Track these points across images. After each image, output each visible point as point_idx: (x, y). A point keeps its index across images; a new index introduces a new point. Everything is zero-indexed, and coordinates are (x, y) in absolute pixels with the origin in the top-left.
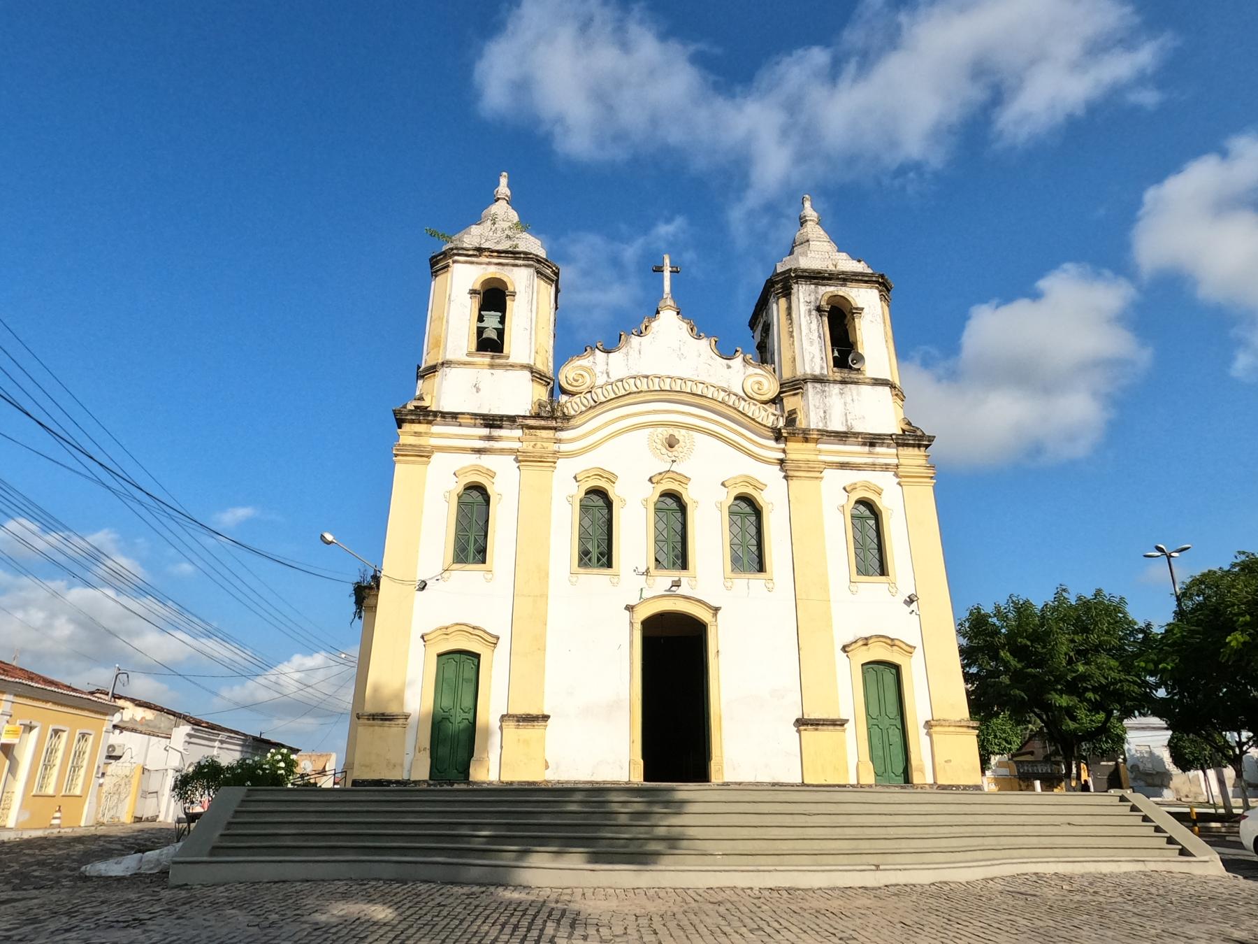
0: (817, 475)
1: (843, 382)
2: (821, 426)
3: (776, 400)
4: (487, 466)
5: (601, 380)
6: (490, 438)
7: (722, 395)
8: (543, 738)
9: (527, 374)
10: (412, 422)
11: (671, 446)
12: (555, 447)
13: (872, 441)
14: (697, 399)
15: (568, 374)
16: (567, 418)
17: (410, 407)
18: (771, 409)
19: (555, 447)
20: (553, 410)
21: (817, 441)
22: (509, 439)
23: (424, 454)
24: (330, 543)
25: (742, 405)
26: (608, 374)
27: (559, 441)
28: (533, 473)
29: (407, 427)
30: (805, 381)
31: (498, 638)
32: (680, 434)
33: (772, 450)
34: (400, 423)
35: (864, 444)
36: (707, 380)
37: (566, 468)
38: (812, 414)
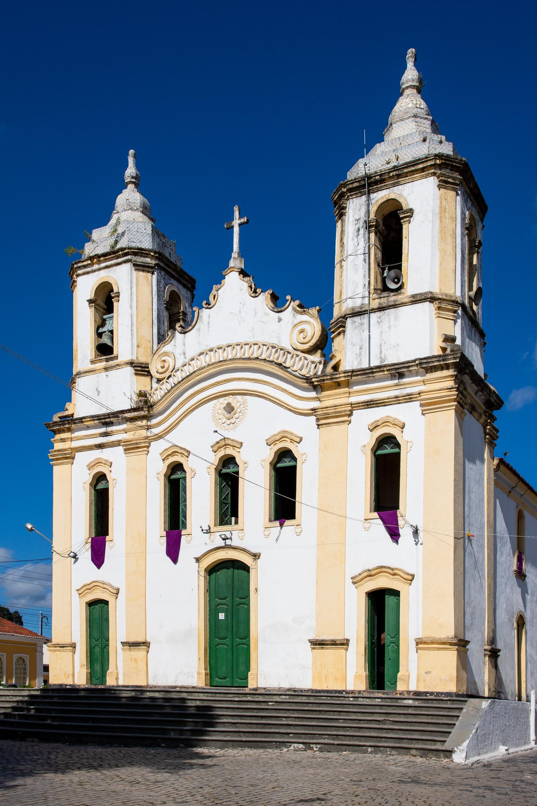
0: (346, 418)
1: (381, 309)
2: (355, 367)
6: (106, 434)
9: (130, 370)
13: (398, 371)
17: (56, 418)
18: (317, 357)
21: (348, 384)
22: (118, 432)
27: (148, 428)
29: (58, 437)
30: (345, 317)
33: (307, 400)
35: (393, 377)
36: (260, 339)
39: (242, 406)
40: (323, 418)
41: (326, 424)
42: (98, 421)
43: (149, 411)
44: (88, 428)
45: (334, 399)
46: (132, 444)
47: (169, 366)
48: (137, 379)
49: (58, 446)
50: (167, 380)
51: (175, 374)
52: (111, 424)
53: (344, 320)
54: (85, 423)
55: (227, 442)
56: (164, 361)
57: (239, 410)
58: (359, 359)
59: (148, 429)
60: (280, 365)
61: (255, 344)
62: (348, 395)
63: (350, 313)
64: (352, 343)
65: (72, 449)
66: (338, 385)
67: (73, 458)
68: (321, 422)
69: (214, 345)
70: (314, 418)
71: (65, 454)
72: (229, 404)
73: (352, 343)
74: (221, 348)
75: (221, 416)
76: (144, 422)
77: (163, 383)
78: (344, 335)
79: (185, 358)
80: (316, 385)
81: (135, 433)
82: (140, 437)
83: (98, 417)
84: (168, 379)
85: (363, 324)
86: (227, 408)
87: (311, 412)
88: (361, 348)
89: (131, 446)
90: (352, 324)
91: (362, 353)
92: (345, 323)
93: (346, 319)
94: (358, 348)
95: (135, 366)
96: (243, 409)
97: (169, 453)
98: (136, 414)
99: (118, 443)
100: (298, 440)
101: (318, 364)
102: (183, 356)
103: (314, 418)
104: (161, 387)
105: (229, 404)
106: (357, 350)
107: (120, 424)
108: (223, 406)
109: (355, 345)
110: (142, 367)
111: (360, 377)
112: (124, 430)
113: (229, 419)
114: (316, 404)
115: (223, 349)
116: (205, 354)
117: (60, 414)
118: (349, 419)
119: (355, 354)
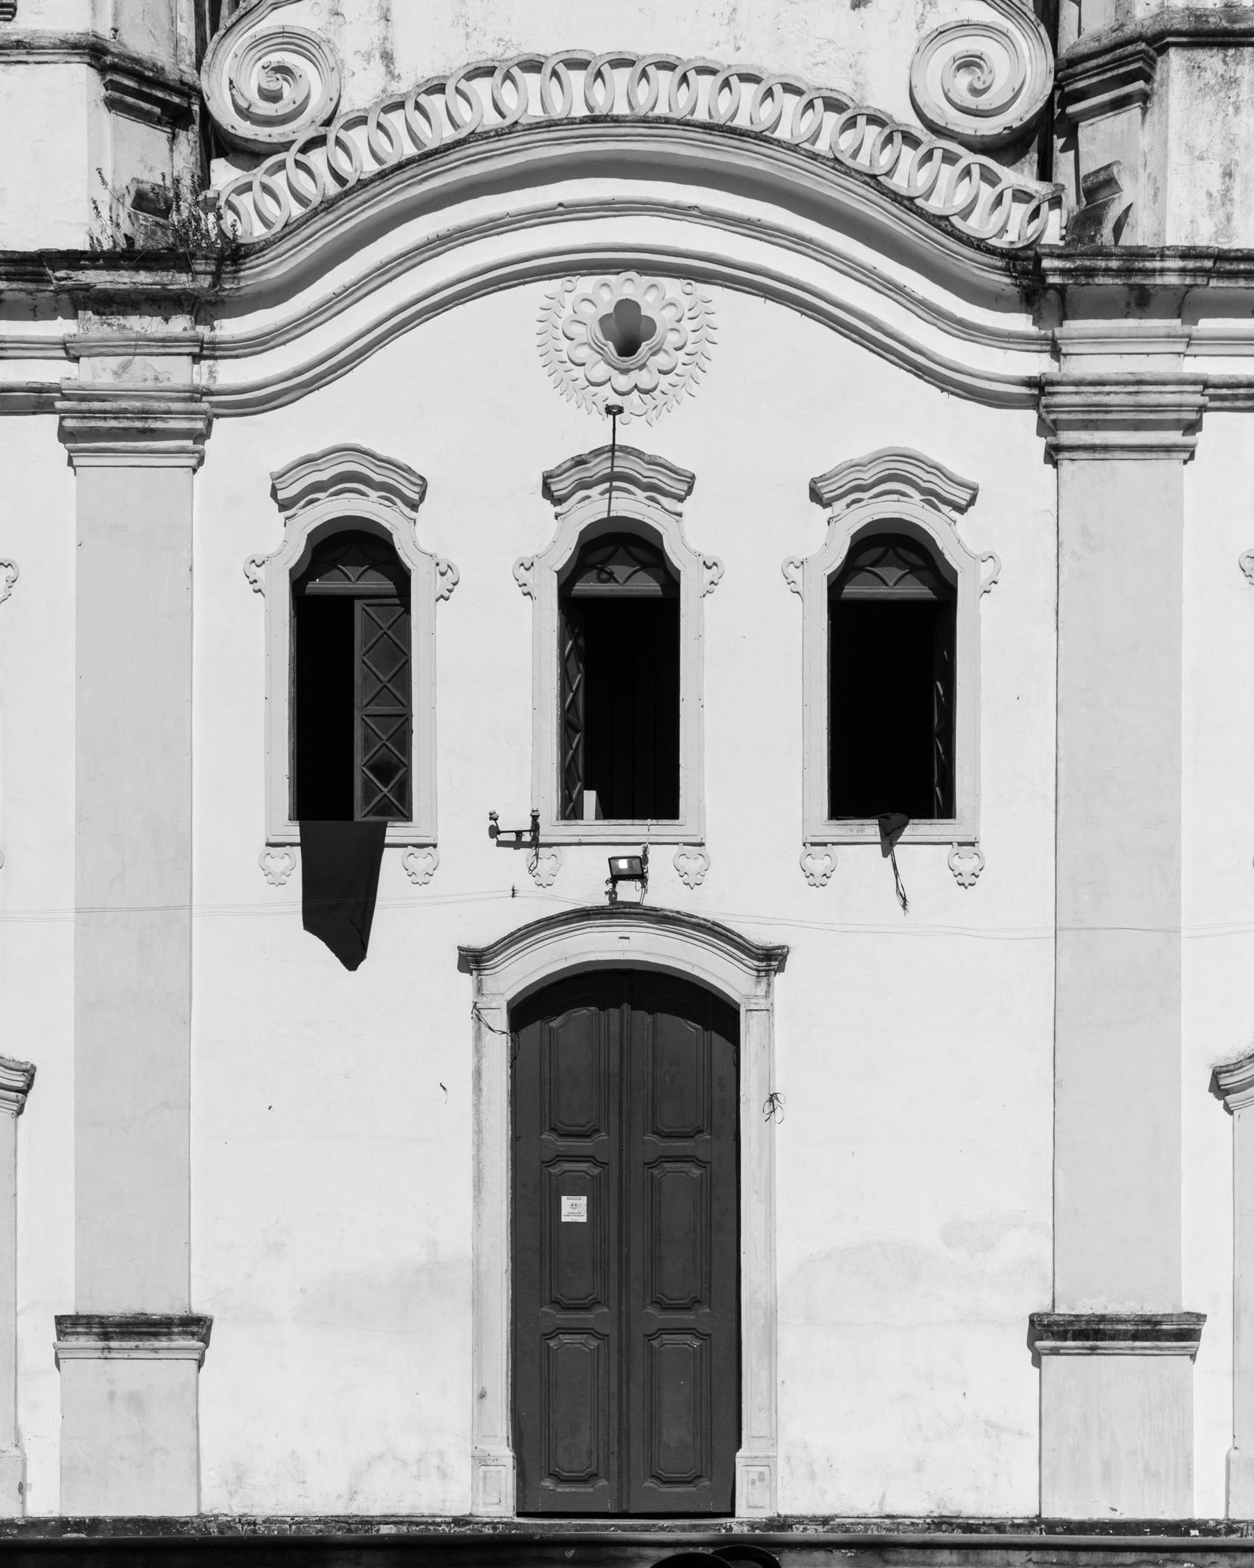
0: (1175, 437)
3: (1042, 135)
5: (361, 93)
7: (829, 134)
11: (628, 347)
12: (200, 375)
14: (720, 159)
15: (231, 82)
16: (234, 254)
18: (1022, 176)
19: (200, 375)
21: (1182, 305)
25: (909, 175)
26: (387, 57)
27: (204, 352)
28: (124, 479)
30: (1158, 42)
32: (658, 298)
36: (772, 65)
37: (248, 451)
38: (1176, 190)
39: (687, 325)
40: (1065, 422)
41: (1092, 448)
43: (217, 277)
45: (1108, 352)
46: (117, 414)
47: (308, 97)
48: (115, 128)
50: (300, 157)
51: (343, 135)
53: (1152, 52)
55: (624, 464)
56: (283, 70)
57: (673, 339)
58: (1221, 213)
59: (197, 358)
60: (872, 180)
61: (746, 78)
62: (1181, 348)
63: (1185, 27)
64: (1190, 148)
66: (1141, 301)
68: (1067, 437)
69: (547, 45)
70: (1031, 416)
72: (627, 308)
73: (1190, 148)
74: (582, 65)
75: (583, 353)
76: (180, 324)
77: (281, 166)
78: (1145, 111)
79: (394, 77)
80: (1030, 282)
81: (125, 367)
82: (150, 384)
84: (304, 149)
85: (1234, 82)
86: (612, 323)
87: (1024, 390)
88: (1228, 174)
90: (1189, 73)
91: (1236, 193)
92: (1152, 63)
93: (1163, 50)
94: (1217, 171)
95: (114, 68)
96: (692, 337)
97: (324, 476)
98: (144, 278)
100: (963, 496)
101: (1045, 206)
102: (378, 65)
103: (1031, 416)
104: (267, 180)
105: (627, 308)
106: (1216, 186)
107: (35, 313)
108: (592, 314)
109: (1201, 159)
110: (139, 77)
111: (1242, 283)
112: (64, 345)
113: (625, 371)
114: (1038, 364)
115: (592, 69)
116: (499, 75)
118: (1188, 440)
119: (1203, 192)
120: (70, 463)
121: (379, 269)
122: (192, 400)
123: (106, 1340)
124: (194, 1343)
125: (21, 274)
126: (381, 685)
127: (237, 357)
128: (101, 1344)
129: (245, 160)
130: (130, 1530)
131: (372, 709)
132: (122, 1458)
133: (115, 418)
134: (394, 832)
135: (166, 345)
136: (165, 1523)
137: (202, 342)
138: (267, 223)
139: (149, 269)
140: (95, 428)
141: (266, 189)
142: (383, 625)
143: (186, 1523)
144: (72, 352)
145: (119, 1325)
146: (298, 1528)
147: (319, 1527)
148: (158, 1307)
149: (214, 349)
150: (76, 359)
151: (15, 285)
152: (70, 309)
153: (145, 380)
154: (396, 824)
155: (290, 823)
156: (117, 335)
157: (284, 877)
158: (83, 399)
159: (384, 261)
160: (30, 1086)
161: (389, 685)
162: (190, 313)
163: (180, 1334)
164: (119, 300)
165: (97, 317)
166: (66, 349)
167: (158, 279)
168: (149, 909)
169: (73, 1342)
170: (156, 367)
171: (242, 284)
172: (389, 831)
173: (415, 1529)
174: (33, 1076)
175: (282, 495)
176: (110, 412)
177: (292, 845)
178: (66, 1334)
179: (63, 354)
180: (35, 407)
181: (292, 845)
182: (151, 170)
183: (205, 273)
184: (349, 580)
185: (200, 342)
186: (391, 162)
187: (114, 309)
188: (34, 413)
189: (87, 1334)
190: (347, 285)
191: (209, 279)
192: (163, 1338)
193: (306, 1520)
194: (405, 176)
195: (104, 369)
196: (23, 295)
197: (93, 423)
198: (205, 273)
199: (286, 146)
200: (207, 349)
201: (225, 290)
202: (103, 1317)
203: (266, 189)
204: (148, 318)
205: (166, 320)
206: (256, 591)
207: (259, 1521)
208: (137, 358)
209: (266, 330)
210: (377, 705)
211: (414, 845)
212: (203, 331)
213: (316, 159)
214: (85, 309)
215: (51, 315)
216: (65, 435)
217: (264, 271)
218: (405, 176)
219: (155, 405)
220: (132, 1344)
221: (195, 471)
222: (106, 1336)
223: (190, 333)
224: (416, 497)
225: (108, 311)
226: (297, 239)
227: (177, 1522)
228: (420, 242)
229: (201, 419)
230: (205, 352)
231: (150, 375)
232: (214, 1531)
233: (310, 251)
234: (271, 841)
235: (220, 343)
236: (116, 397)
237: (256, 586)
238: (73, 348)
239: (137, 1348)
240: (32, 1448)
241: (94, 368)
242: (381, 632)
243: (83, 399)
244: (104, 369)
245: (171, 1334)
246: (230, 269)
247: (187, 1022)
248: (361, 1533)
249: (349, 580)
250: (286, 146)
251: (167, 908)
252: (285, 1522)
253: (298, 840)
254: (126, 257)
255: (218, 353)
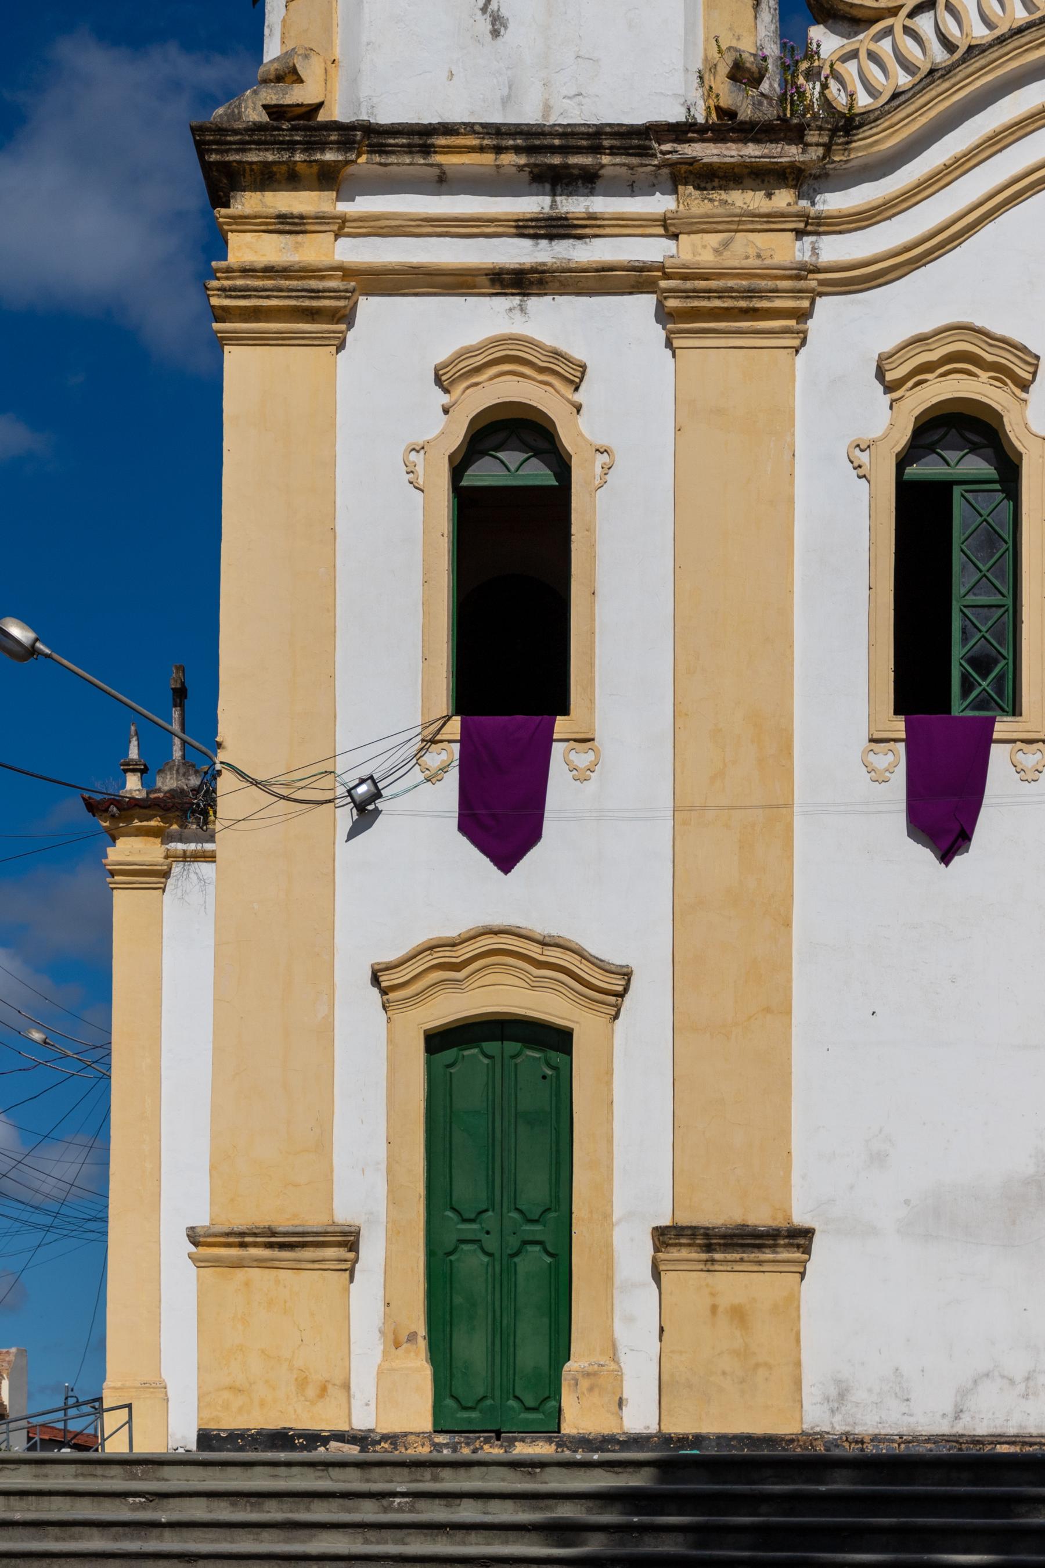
4: (548, 339)
6: (555, 228)
8: (789, 1310)
10: (267, 179)
17: (253, 111)
20: (791, 94)
23: (320, 309)
24: (31, 651)
27: (811, 226)
28: (724, 362)
29: (248, 202)
31: (627, 975)
34: (222, 183)
42: (522, 160)
44: (443, 183)
46: (721, 293)
49: (247, 249)
52: (588, 181)
54: (439, 159)
59: (800, 234)
65: (347, 272)
67: (347, 317)
71: (316, 294)
76: (783, 199)
77: (889, 31)
81: (726, 244)
82: (752, 262)
83: (530, 139)
84: (911, 15)
89: (717, 303)
99: (637, 279)
104: (873, 47)
107: (632, 189)
117: (271, 96)
120: (669, 344)
121: (991, 138)
122: (798, 278)
123: (708, 1252)
124: (798, 1255)
125: (626, 148)
126: (979, 575)
127: (840, 232)
128: (704, 1256)
129: (845, 27)
130: (734, 1447)
131: (971, 599)
132: (724, 1373)
133: (719, 297)
134: (1002, 728)
135: (770, 222)
136: (770, 1440)
137: (808, 217)
138: (872, 91)
139: (757, 141)
140: (693, 308)
141: (873, 56)
142: (982, 512)
143: (792, 1441)
144: (672, 229)
145: (724, 1236)
146: (907, 1448)
147: (929, 1446)
148: (761, 1217)
149: (819, 225)
150: (675, 236)
151: (618, 160)
152: (669, 184)
153: (747, 257)
154: (1005, 719)
155: (895, 718)
156: (721, 210)
157: (887, 774)
158: (685, 277)
159: (997, 131)
160: (626, 989)
161: (989, 575)
162: (794, 187)
163: (785, 1246)
164: (721, 174)
165: (698, 192)
166: (665, 227)
167: (766, 151)
168: (751, 807)
169: (674, 1254)
170: (759, 244)
171: (852, 156)
172: (998, 726)
173: (1028, 1449)
174: (629, 980)
175: (890, 376)
176: (715, 291)
177: (896, 740)
178: (668, 1245)
179: (661, 231)
180: (633, 287)
181: (896, 740)
182: (739, 39)
183: (818, 145)
184: (948, 465)
185: (805, 217)
186: (1003, 29)
187: (716, 183)
188: (631, 293)
189: (689, 1245)
190: (958, 156)
191: (820, 151)
192: (767, 1251)
193: (915, 1439)
194: (1024, 40)
195: (704, 247)
196: (624, 169)
197: (696, 303)
198: (818, 145)
199: (894, 11)
200: (812, 224)
201: (834, 162)
202: (708, 1228)
203: (873, 56)
204: (751, 193)
205: (769, 196)
206: (859, 477)
207: (867, 1439)
208: (739, 235)
209: (874, 204)
210: (975, 595)
211: (1023, 741)
212: (804, 203)
213: (924, 23)
214: (686, 184)
215: (649, 190)
216: (663, 315)
217: (876, 142)
218: (1024, 40)
219: (763, 284)
220: (737, 1256)
221: (797, 352)
222: (709, 1248)
223: (793, 209)
224: (1029, 377)
225: (709, 186)
226: (912, 108)
227: (783, 1439)
228: (1034, 111)
229: (807, 298)
230: (809, 228)
231: (752, 252)
232: (821, 1449)
233: (923, 120)
234: (877, 735)
235: (825, 218)
236: (720, 276)
237: (861, 472)
238: (673, 225)
239: (742, 1260)
240: (628, 1363)
241: (694, 245)
242: (980, 519)
243: (685, 277)
244: (704, 247)
245: (775, 1246)
246: (842, 140)
247: (788, 924)
248: (974, 1452)
249: (948, 465)
250: (894, 11)
251: (770, 807)
252: (893, 1441)
253: (903, 735)
254: (726, 125)
255: (822, 229)
